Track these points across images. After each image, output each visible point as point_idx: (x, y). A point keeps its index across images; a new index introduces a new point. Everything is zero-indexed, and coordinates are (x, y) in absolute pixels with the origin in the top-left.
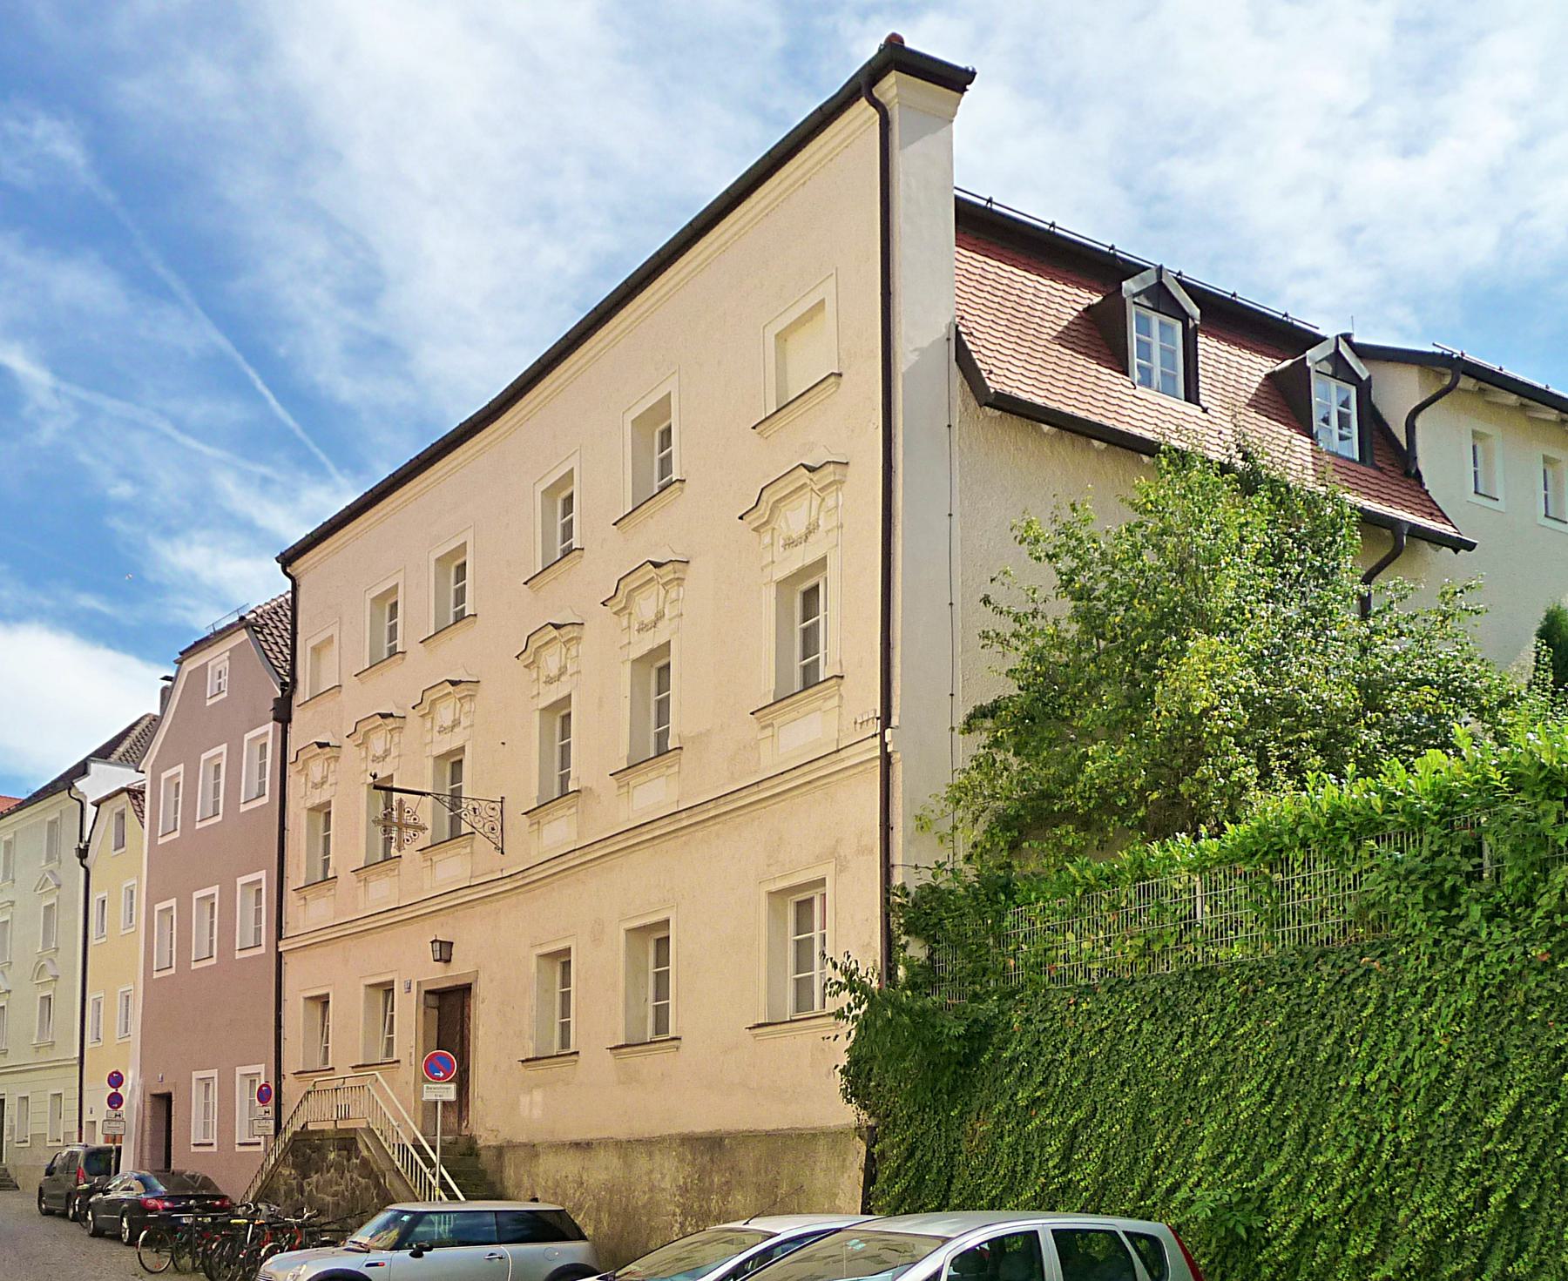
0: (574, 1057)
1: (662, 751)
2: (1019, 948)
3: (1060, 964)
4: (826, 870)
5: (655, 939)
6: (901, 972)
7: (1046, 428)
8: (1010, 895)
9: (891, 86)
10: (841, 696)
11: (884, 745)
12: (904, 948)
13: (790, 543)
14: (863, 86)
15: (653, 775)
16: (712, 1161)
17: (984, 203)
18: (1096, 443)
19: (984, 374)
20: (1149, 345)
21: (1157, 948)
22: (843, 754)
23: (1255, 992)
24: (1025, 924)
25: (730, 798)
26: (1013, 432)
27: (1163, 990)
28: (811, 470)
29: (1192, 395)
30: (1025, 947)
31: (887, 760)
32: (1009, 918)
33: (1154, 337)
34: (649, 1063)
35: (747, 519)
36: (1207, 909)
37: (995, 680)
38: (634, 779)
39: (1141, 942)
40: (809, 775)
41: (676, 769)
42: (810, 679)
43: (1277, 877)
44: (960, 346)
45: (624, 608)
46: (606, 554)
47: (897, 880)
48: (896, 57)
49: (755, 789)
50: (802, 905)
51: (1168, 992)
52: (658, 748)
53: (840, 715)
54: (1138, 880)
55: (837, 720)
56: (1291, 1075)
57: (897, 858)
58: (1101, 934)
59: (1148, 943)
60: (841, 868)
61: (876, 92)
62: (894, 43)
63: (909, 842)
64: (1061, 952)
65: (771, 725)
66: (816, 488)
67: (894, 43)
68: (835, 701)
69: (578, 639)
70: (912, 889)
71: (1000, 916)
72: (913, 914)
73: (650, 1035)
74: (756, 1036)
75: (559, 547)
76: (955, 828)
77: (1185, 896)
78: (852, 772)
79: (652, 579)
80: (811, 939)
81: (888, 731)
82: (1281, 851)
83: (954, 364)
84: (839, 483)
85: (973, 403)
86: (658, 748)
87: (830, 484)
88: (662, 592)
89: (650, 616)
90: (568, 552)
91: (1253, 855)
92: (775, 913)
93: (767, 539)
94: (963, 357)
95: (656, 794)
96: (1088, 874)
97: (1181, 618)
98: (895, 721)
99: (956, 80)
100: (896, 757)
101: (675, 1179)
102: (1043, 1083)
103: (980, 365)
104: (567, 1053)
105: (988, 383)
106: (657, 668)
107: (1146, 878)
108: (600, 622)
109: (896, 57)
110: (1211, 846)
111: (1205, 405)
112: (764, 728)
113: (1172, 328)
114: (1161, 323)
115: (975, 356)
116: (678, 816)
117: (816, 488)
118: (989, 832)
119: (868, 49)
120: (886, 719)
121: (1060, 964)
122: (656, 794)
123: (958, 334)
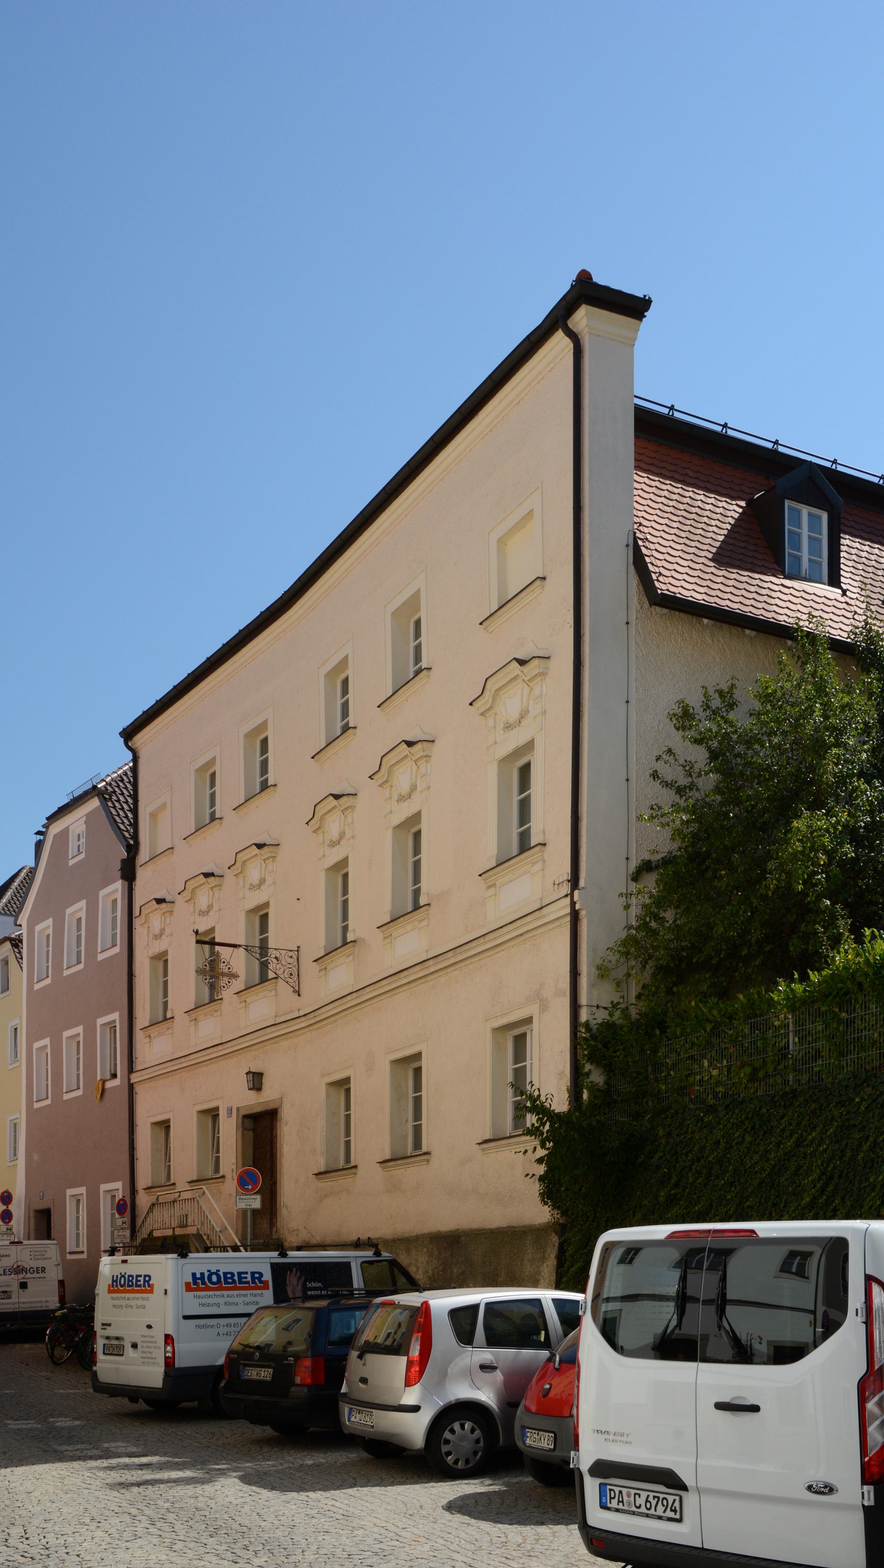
0: (353, 1170)
1: (417, 907)
2: (669, 1074)
3: (697, 1088)
4: (532, 1010)
5: (410, 1066)
6: (585, 1096)
7: (706, 621)
8: (663, 1030)
9: (583, 318)
10: (544, 861)
11: (573, 904)
12: (588, 1074)
13: (508, 727)
14: (558, 319)
15: (408, 928)
16: (452, 1254)
17: (666, 411)
18: (747, 632)
19: (654, 576)
20: (799, 535)
21: (761, 1074)
22: (545, 911)
23: (821, 1109)
24: (674, 1055)
25: (464, 948)
26: (679, 625)
27: (760, 1108)
28: (522, 662)
29: (834, 580)
30: (672, 1073)
31: (575, 916)
32: (663, 1050)
33: (805, 523)
34: (410, 1173)
35: (476, 704)
36: (797, 1040)
37: (660, 841)
38: (397, 930)
39: (748, 1070)
40: (519, 927)
41: (425, 923)
42: (524, 845)
43: (844, 1015)
44: (637, 549)
45: (386, 781)
46: (375, 731)
47: (584, 1016)
48: (586, 292)
49: (482, 940)
50: (517, 1038)
51: (764, 1110)
52: (413, 905)
53: (543, 877)
54: (749, 1018)
55: (540, 880)
56: (840, 1177)
57: (583, 999)
58: (725, 1062)
59: (755, 1070)
60: (544, 1007)
61: (571, 323)
62: (584, 278)
63: (592, 986)
64: (698, 1078)
65: (494, 885)
66: (526, 679)
67: (584, 278)
68: (539, 866)
69: (352, 807)
70: (593, 1023)
71: (655, 1051)
72: (591, 1045)
73: (410, 1150)
74: (484, 1150)
75: (339, 725)
76: (629, 975)
77: (782, 1031)
78: (551, 926)
79: (406, 756)
80: (525, 1066)
81: (576, 892)
82: (846, 994)
83: (632, 569)
84: (543, 674)
85: (646, 604)
86: (413, 905)
87: (535, 676)
88: (415, 768)
89: (405, 788)
90: (346, 728)
91: (827, 996)
92: (498, 1046)
93: (491, 723)
94: (639, 562)
95: (411, 943)
96: (715, 1012)
97: (802, 790)
98: (582, 883)
99: (634, 307)
100: (583, 913)
101: (426, 1272)
102: (677, 1185)
103: (651, 567)
104: (350, 1168)
105: (657, 584)
106: (411, 832)
107: (756, 1016)
108: (368, 791)
109: (586, 292)
110: (798, 988)
111: (844, 587)
112: (489, 887)
113: (819, 518)
114: (810, 514)
115: (647, 560)
116: (427, 963)
117: (526, 679)
118: (654, 975)
119: (562, 287)
120: (574, 881)
121: (697, 1088)
122: (411, 943)
123: (635, 539)
